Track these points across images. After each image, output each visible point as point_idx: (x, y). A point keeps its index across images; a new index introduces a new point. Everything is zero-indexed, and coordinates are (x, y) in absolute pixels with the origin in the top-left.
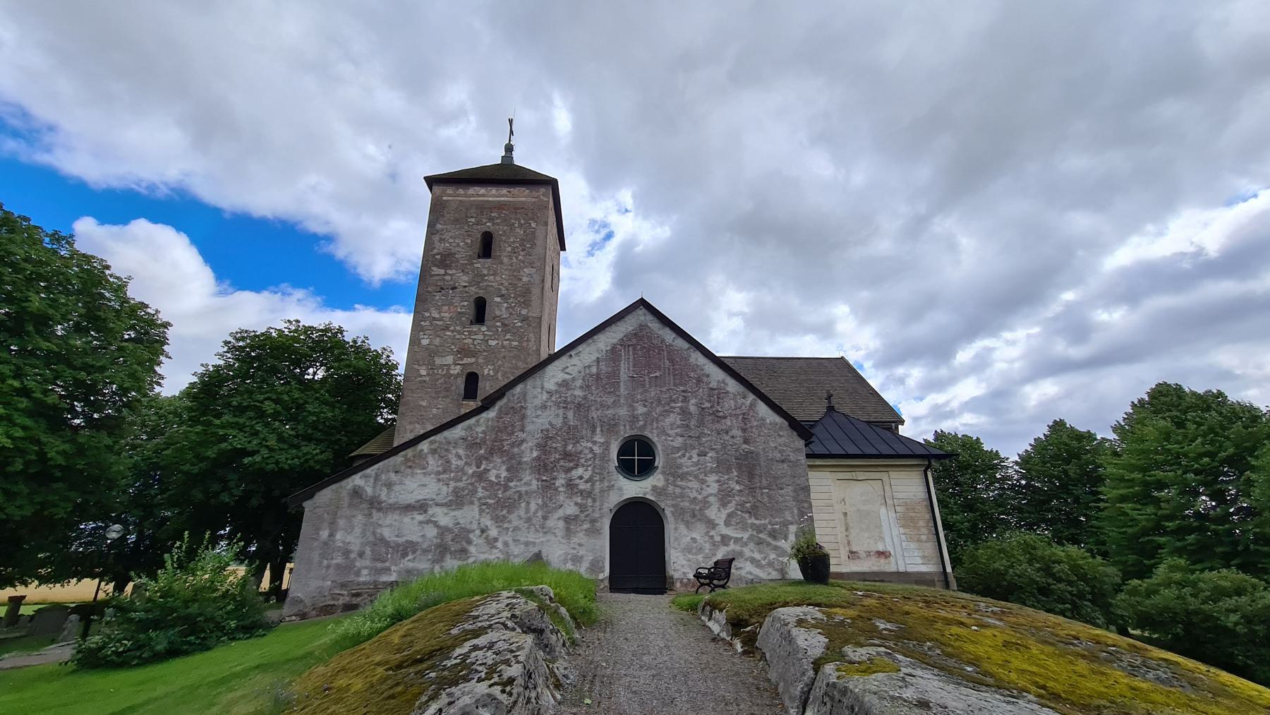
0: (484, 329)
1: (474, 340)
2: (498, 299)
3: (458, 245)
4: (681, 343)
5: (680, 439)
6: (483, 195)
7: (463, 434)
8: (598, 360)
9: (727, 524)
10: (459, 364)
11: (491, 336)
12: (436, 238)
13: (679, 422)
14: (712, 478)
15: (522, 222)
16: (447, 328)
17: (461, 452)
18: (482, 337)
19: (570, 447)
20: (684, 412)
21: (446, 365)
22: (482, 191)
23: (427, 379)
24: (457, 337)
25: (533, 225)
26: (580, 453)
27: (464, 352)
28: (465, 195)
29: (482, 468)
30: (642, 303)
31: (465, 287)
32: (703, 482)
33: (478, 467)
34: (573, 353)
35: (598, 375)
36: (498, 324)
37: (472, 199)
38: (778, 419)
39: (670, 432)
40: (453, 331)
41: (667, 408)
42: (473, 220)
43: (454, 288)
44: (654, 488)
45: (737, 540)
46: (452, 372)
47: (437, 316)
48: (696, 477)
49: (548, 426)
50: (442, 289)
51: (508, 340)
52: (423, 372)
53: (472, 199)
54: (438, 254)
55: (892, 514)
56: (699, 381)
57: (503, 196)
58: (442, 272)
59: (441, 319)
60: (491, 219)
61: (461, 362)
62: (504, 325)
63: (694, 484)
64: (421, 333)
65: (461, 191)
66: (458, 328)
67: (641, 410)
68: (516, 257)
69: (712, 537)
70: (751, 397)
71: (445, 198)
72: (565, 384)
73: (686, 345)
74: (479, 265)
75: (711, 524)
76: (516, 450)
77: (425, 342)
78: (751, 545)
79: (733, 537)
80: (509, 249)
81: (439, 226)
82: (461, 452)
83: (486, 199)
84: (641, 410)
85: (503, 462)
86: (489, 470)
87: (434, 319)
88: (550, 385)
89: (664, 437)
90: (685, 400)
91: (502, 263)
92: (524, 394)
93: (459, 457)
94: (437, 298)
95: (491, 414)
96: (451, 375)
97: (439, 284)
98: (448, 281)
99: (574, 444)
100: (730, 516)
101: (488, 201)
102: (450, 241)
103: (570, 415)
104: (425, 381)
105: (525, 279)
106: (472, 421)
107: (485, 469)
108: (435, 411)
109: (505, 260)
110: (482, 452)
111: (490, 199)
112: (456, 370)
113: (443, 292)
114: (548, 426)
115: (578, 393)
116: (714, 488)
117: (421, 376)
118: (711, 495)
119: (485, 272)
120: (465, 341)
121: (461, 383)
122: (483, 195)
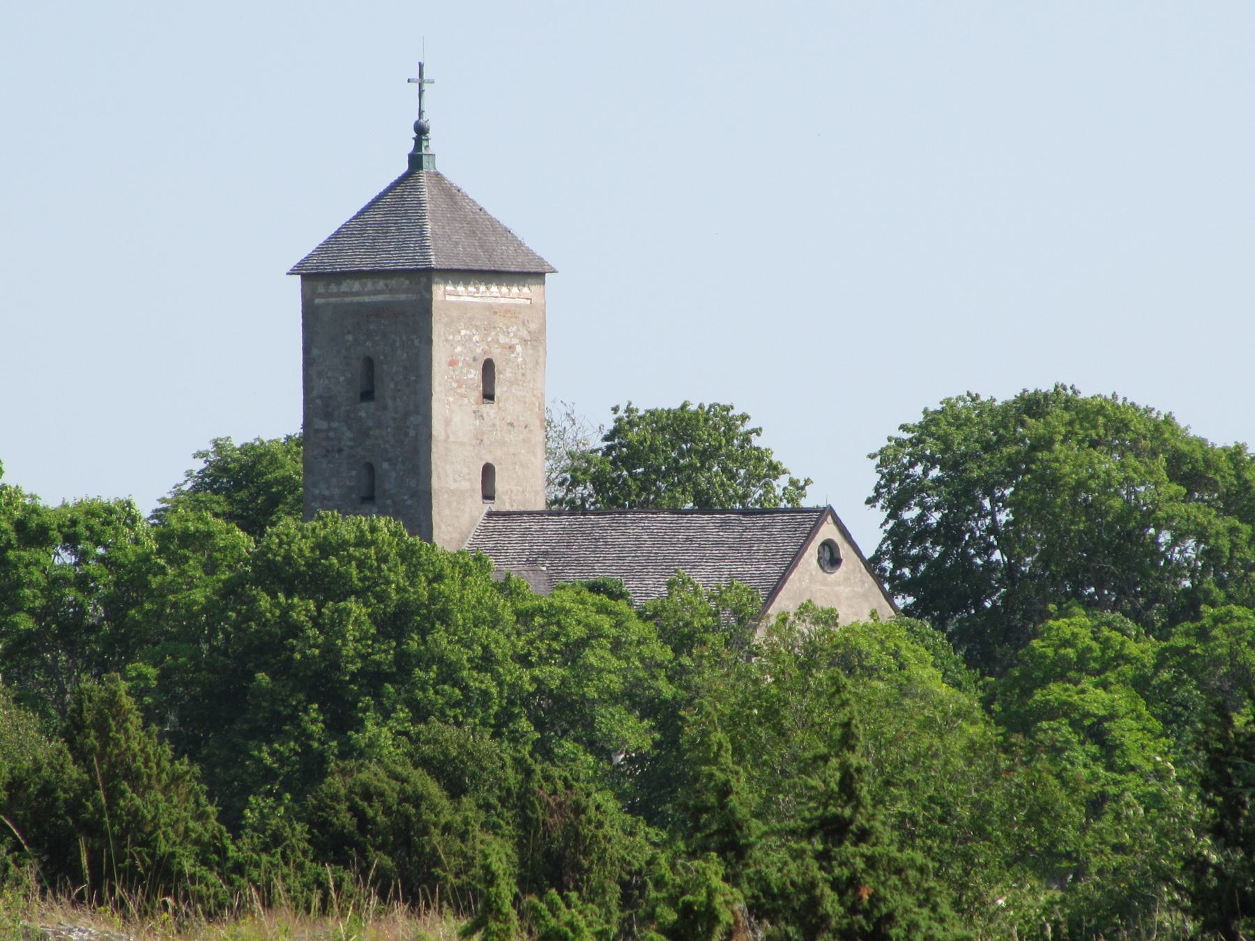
6: (357, 294)
25: (416, 343)
28: (338, 295)
31: (351, 447)
42: (350, 338)
43: (340, 451)
47: (327, 493)
50: (328, 451)
53: (348, 300)
74: (363, 414)
80: (392, 385)
81: (315, 352)
91: (385, 408)
105: (412, 433)
109: (390, 403)
111: (367, 299)
119: (370, 423)
122: (357, 294)
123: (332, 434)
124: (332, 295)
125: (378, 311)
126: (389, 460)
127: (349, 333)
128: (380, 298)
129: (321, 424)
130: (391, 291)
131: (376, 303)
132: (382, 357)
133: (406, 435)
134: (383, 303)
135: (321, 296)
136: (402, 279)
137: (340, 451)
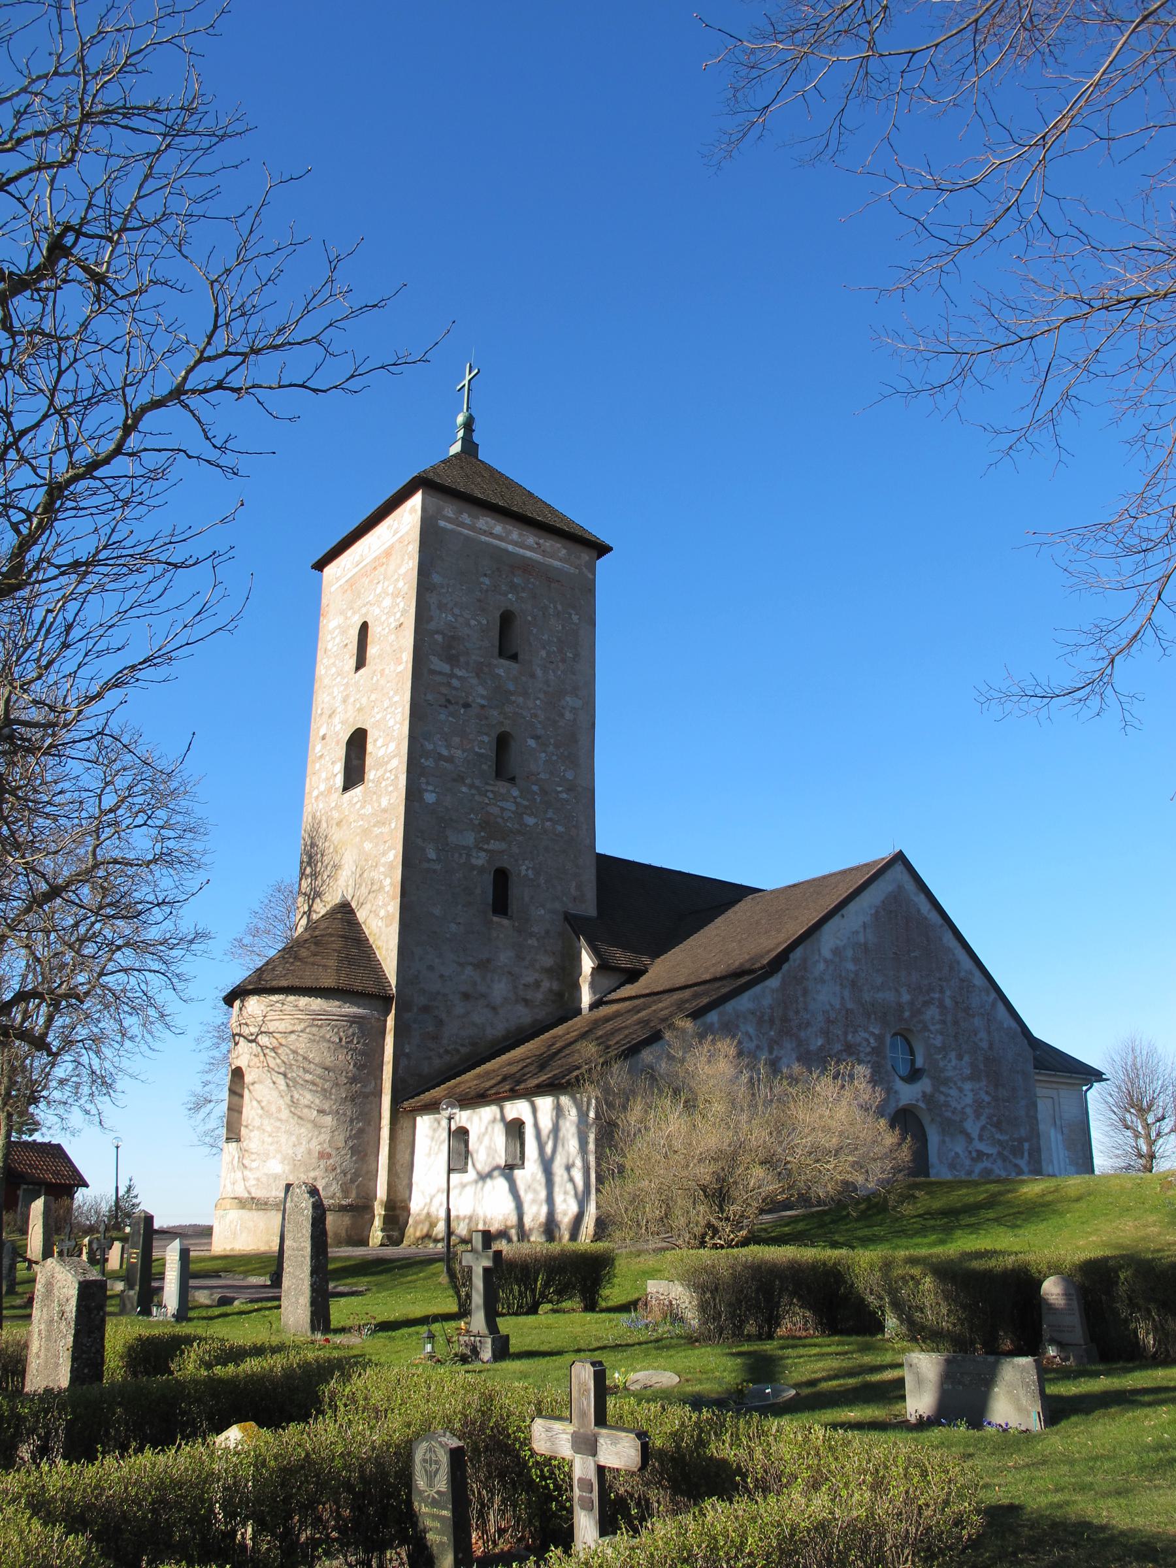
0: (515, 792)
1: (503, 809)
2: (532, 743)
3: (468, 625)
4: (934, 917)
5: (939, 1037)
7: (750, 1005)
8: (865, 926)
9: (981, 1138)
10: (481, 849)
11: (526, 807)
12: (433, 599)
13: (937, 1017)
14: (968, 1086)
15: (559, 607)
16: (460, 779)
17: (751, 1030)
18: (514, 808)
19: (850, 1037)
20: (942, 1005)
21: (464, 848)
22: (498, 529)
23: (438, 867)
24: (477, 798)
25: (575, 618)
26: (859, 1045)
27: (490, 828)
28: (472, 528)
29: (775, 1053)
30: (900, 858)
31: (483, 707)
32: (961, 1090)
33: (771, 1052)
34: (844, 911)
35: (866, 944)
36: (535, 788)
37: (483, 538)
38: (1014, 1025)
39: (932, 1028)
40: (472, 786)
41: (927, 998)
44: (924, 1094)
45: (988, 1156)
46: (474, 861)
47: (445, 752)
48: (955, 1084)
49: (828, 1007)
50: (449, 701)
51: (550, 820)
52: (432, 854)
53: (483, 538)
54: (437, 632)
55: (1060, 1137)
56: (951, 968)
57: (529, 548)
58: (446, 668)
59: (450, 759)
60: (513, 587)
61: (486, 847)
62: (544, 792)
63: (954, 1092)
64: (423, 780)
65: (466, 518)
66: (477, 782)
67: (906, 998)
68: (554, 672)
69: (970, 1152)
70: (993, 995)
71: (442, 523)
72: (837, 951)
73: (940, 921)
74: (501, 672)
75: (969, 1138)
76: (802, 1034)
77: (430, 798)
78: (999, 1162)
79: (985, 1154)
80: (543, 653)
81: (436, 579)
82: (751, 1030)
83: (503, 545)
84: (906, 998)
85: (793, 1050)
86: (781, 1058)
87: (441, 757)
88: (826, 953)
89: (926, 1034)
90: (942, 991)
91: (533, 676)
92: (805, 960)
93: (751, 1038)
94: (443, 717)
95: (774, 982)
96: (473, 867)
97: (444, 690)
98: (455, 689)
99: (853, 1033)
100: (983, 1128)
101: (506, 551)
102: (457, 611)
103: (846, 993)
104: (435, 871)
106: (757, 989)
107: (776, 1057)
108: (453, 927)
109: (539, 673)
110: (772, 1033)
111: (510, 548)
112: (480, 860)
113: (451, 708)
114: (828, 1007)
115: (851, 966)
116: (969, 1099)
117: (429, 860)
118: (966, 1106)
119: (511, 687)
120: (489, 808)
121: (486, 883)
123: (455, 682)
124: (462, 525)
125: (526, 567)
126: (537, 738)
127: (485, 575)
128: (528, 554)
129: (437, 664)
130: (544, 553)
131: (523, 557)
132: (529, 618)
133: (562, 715)
134: (530, 559)
135: (448, 520)
136: (559, 545)
137: (467, 706)
